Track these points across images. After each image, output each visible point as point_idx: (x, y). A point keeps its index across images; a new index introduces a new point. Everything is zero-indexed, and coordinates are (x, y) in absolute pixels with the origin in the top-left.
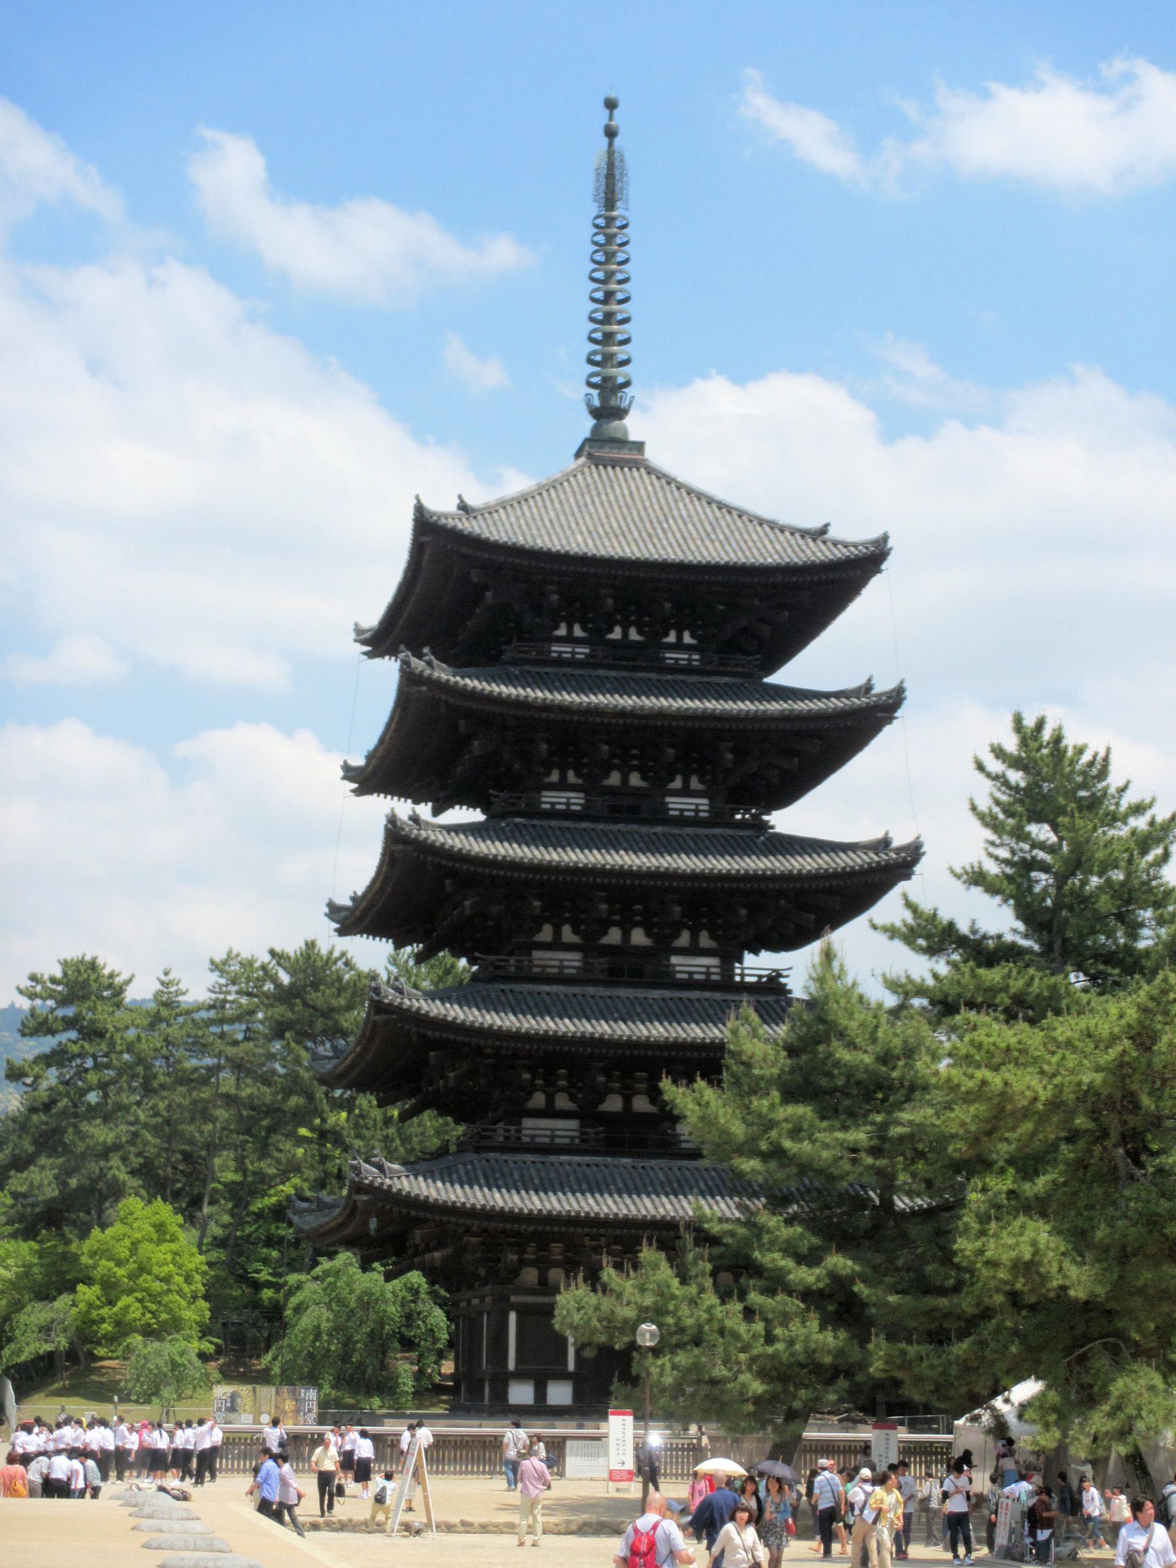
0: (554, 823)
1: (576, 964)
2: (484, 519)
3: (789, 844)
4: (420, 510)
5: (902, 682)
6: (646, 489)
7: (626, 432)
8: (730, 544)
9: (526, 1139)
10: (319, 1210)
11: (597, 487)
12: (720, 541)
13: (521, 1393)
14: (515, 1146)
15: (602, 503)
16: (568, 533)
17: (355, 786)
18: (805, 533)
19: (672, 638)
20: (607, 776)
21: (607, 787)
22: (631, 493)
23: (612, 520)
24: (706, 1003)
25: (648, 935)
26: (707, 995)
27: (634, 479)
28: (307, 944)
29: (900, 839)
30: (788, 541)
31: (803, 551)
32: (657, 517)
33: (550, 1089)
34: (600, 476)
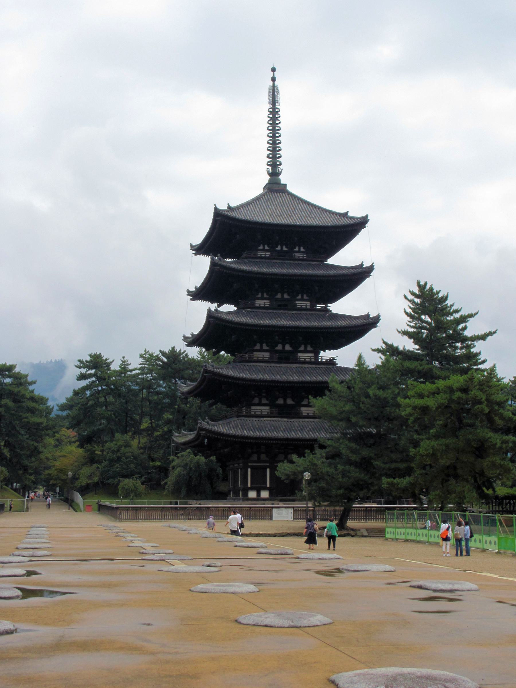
0: (260, 310)
1: (268, 356)
2: (236, 211)
3: (336, 316)
4: (216, 209)
5: (373, 263)
6: (287, 200)
7: (280, 180)
8: (316, 219)
9: (253, 413)
10: (183, 436)
11: (271, 200)
12: (313, 218)
13: (252, 494)
14: (249, 415)
15: (274, 205)
16: (264, 216)
17: (191, 297)
18: (340, 215)
19: (297, 249)
20: (277, 294)
21: (276, 298)
22: (283, 201)
23: (278, 211)
24: (310, 368)
25: (291, 346)
26: (310, 366)
27: (283, 196)
28: (172, 348)
30: (335, 217)
31: (340, 221)
32: (292, 210)
34: (272, 196)
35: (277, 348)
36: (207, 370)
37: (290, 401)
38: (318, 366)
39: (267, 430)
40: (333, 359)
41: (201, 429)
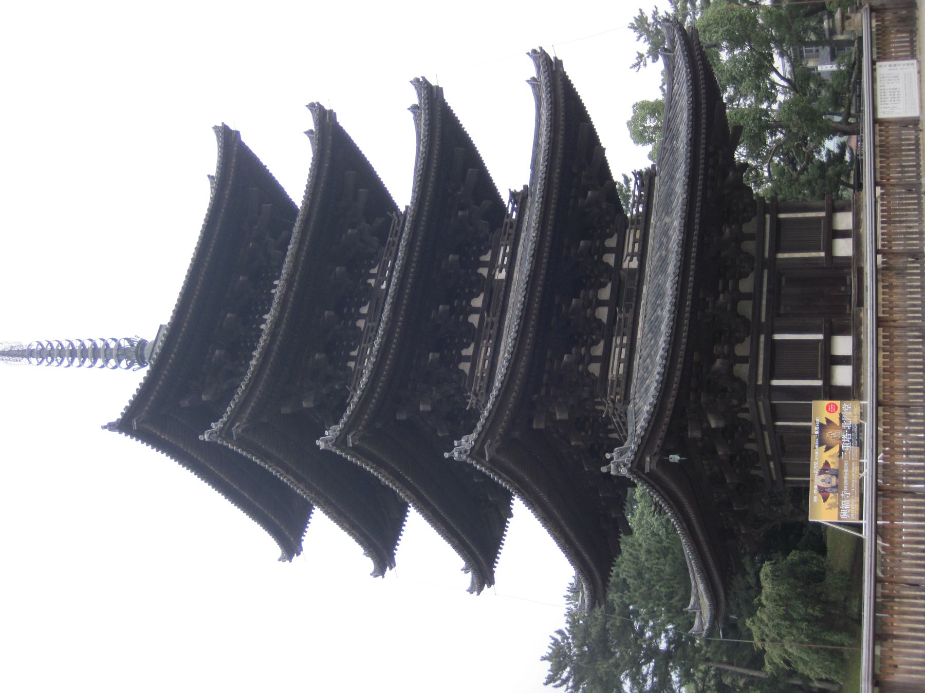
4: (111, 427)
20: (359, 328)
25: (477, 296)
29: (413, 98)
33: (586, 360)
35: (476, 325)
36: (472, 449)
37: (605, 294)
38: (524, 227)
39: (661, 310)
40: (513, 195)
41: (637, 466)
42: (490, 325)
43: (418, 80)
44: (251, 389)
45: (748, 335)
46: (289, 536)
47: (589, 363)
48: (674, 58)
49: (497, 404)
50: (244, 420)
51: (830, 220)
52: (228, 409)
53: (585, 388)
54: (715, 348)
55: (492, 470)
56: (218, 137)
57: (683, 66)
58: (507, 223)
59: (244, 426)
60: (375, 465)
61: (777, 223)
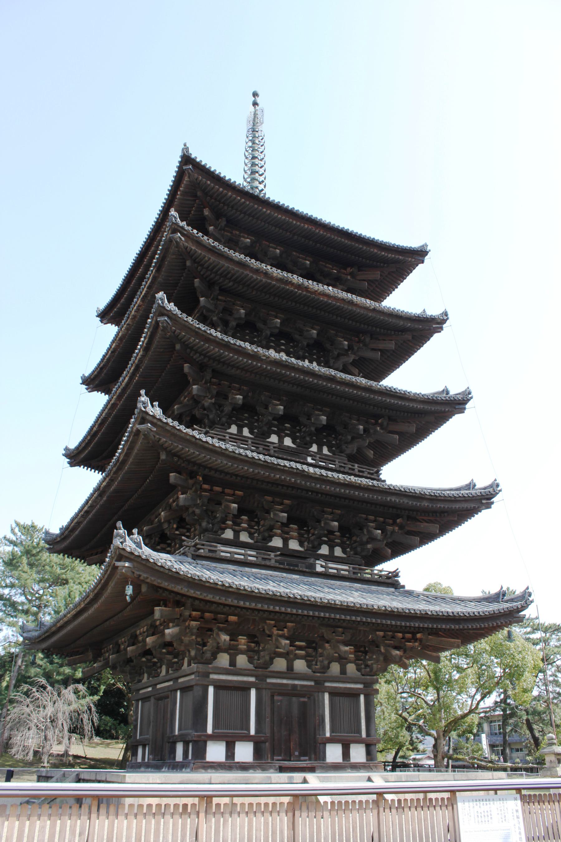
4: (186, 149)
25: (293, 442)
35: (268, 440)
36: (146, 413)
37: (294, 545)
42: (266, 448)
43: (470, 393)
44: (212, 250)
45: (255, 668)
46: (113, 312)
47: (233, 530)
48: (498, 602)
49: (188, 437)
50: (186, 244)
51: (359, 741)
52: (195, 231)
53: (211, 525)
54: (245, 638)
55: (131, 433)
56: (421, 247)
57: (491, 609)
58: (353, 466)
59: (181, 244)
60: (145, 345)
61: (354, 695)
